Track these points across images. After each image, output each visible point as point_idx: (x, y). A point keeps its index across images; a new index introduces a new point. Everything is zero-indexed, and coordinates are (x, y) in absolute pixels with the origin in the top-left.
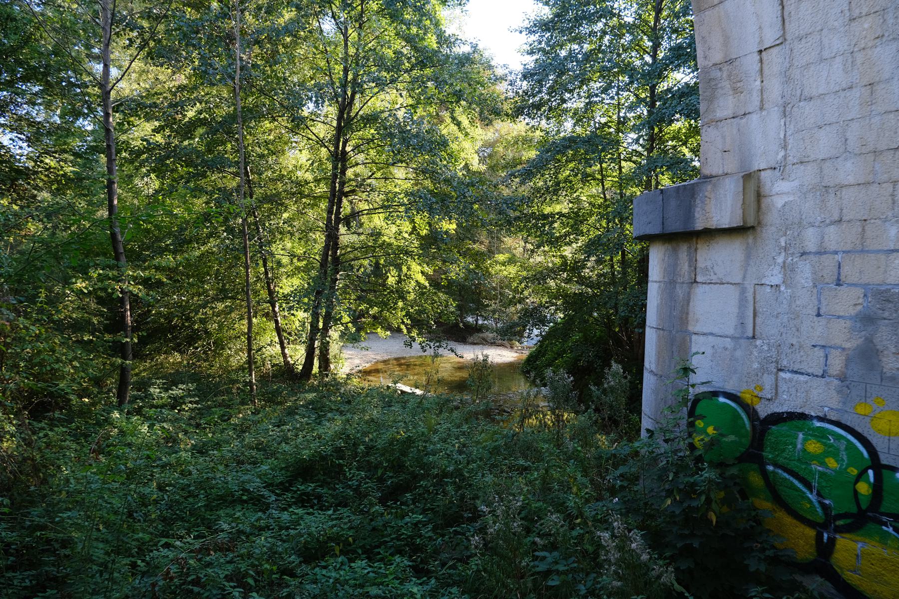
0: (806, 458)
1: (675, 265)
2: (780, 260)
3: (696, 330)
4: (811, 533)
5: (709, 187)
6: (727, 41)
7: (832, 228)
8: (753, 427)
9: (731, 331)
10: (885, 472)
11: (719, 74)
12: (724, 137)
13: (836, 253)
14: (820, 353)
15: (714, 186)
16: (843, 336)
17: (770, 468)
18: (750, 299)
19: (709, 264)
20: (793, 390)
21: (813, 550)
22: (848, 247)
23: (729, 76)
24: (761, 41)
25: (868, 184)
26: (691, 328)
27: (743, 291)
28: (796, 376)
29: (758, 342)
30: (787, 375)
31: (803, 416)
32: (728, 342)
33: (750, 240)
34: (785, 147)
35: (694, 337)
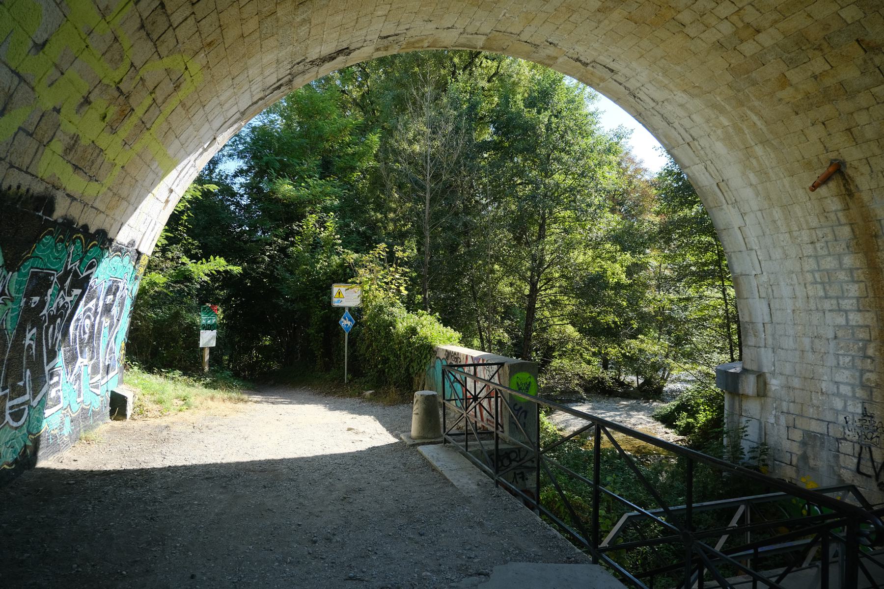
2: (774, 412)
6: (750, 314)
27: (760, 423)
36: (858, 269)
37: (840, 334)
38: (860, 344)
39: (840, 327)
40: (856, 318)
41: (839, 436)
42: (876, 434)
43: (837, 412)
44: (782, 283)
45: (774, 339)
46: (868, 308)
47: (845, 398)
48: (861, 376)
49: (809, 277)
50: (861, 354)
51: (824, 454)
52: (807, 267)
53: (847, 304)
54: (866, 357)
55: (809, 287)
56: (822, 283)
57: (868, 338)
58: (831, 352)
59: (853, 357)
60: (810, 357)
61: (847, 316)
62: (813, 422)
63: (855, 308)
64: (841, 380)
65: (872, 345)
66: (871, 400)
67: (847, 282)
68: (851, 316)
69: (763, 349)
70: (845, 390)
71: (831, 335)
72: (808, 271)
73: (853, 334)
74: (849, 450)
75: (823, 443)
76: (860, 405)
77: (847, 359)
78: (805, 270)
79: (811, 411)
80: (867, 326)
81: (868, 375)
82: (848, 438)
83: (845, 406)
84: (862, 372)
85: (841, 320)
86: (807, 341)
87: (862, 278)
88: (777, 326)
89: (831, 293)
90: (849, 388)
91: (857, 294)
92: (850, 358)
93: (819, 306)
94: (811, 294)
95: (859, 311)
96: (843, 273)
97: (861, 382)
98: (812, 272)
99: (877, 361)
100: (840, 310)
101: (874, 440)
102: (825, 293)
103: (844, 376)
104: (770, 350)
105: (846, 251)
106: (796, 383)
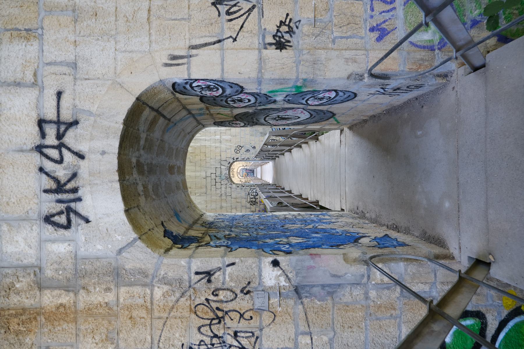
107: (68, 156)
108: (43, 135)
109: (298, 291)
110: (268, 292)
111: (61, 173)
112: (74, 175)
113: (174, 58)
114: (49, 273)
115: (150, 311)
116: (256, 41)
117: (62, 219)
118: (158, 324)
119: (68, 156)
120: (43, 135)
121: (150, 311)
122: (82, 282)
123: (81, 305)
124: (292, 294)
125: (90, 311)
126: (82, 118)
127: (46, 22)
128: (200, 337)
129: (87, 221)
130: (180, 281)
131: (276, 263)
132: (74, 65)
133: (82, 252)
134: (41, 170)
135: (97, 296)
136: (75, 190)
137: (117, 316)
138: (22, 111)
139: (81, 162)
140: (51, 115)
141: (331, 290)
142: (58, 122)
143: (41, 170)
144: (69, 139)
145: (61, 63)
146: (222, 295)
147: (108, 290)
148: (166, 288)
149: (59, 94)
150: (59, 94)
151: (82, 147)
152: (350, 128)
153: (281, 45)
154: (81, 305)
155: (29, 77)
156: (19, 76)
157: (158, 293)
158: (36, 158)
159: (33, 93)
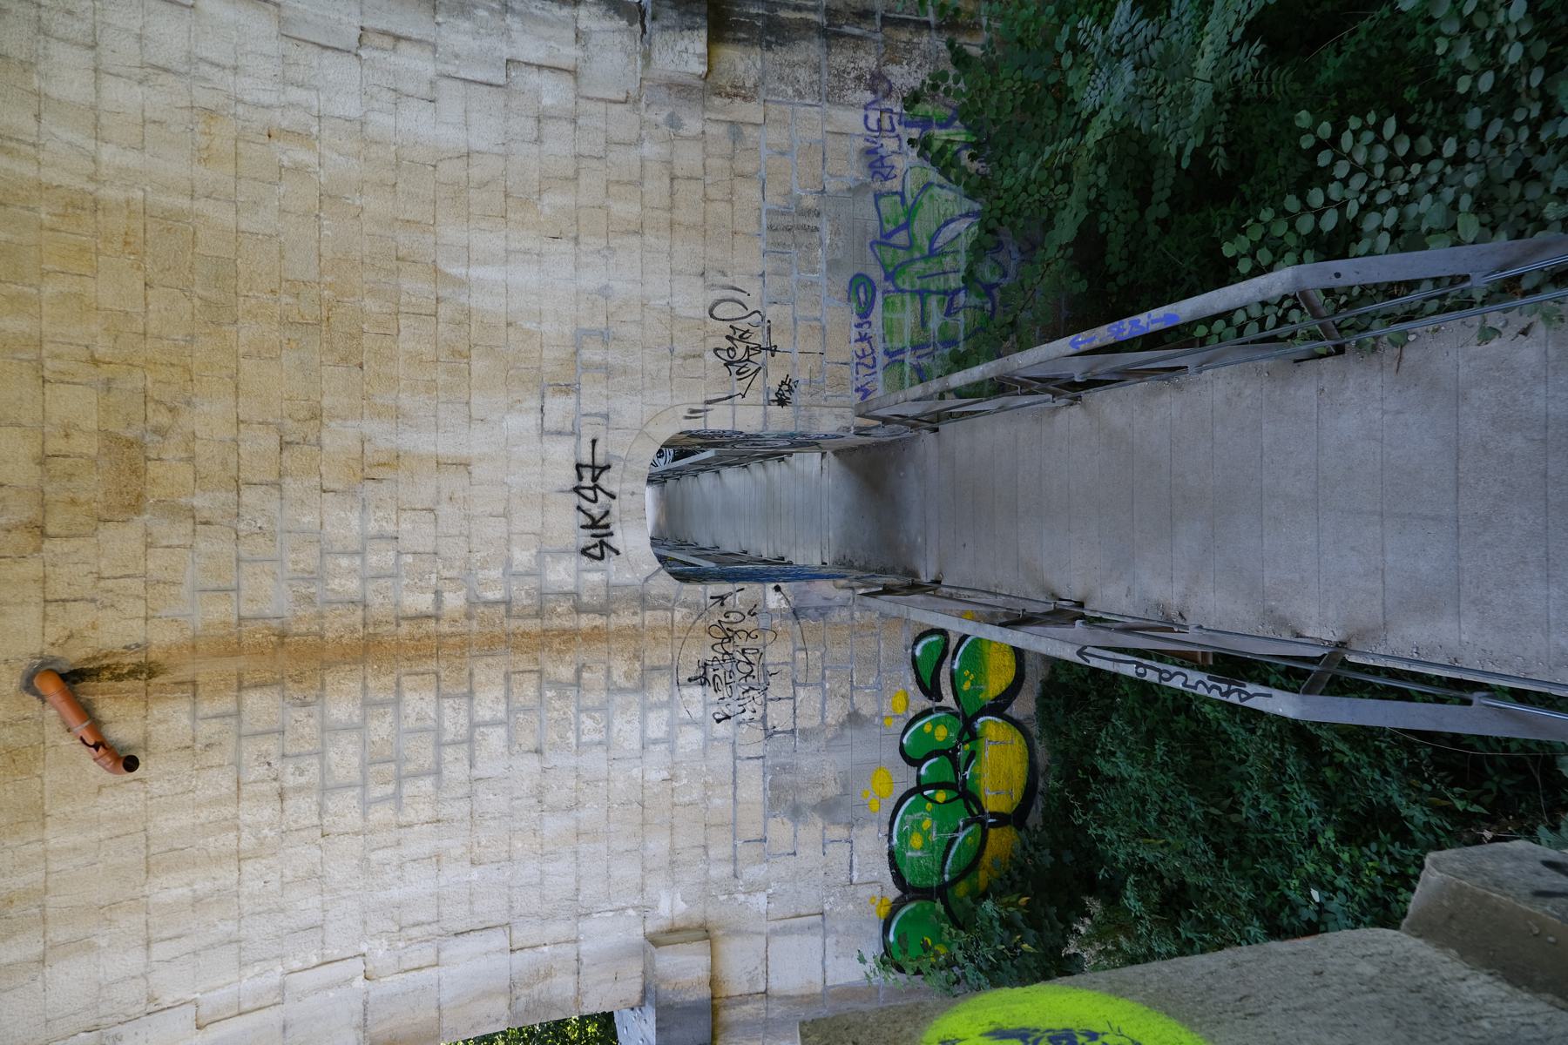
0: (927, 846)
1: (745, 1023)
2: (741, 898)
3: (820, 982)
4: (992, 831)
5: (663, 987)
6: (487, 994)
7: (711, 853)
8: (911, 900)
9: (818, 940)
10: (923, 782)
11: (523, 999)
12: (599, 983)
13: (735, 846)
14: (830, 847)
15: (662, 980)
16: (812, 831)
17: (947, 877)
18: (782, 923)
19: (745, 978)
20: (869, 867)
21: (1007, 829)
22: (730, 836)
23: (529, 986)
24: (501, 951)
25: (672, 827)
26: (819, 989)
27: (775, 932)
28: (855, 866)
29: (827, 908)
30: (855, 874)
31: (891, 855)
32: (830, 940)
33: (719, 933)
34: (624, 909)
35: (829, 983)
36: (365, 687)
37: (530, 742)
38: (549, 694)
39: (510, 741)
40: (489, 703)
41: (760, 734)
42: (738, 656)
43: (709, 740)
44: (396, 893)
45: (551, 917)
46: (465, 673)
47: (674, 726)
48: (621, 690)
49: (381, 814)
50: (572, 693)
51: (806, 763)
52: (353, 819)
53: (454, 721)
54: (577, 682)
55: (410, 815)
56: (400, 780)
57: (534, 676)
58: (573, 762)
59: (580, 710)
60: (590, 814)
61: (486, 724)
62: (743, 794)
63: (463, 703)
64: (637, 735)
65: (549, 668)
66: (670, 668)
67: (398, 717)
68: (484, 713)
69: (584, 947)
70: (657, 725)
71: (533, 762)
72: (364, 815)
73: (526, 710)
74: (786, 707)
75: (783, 768)
76: (685, 691)
77: (588, 723)
78: (359, 823)
79: (720, 801)
80: (507, 677)
81: (618, 676)
82: (760, 712)
83: (693, 723)
84: (612, 689)
85: (495, 739)
86: (555, 825)
87: (389, 680)
88: (518, 909)
89: (426, 759)
90: (652, 716)
91: (430, 696)
92: (583, 717)
93: (461, 792)
94: (426, 812)
95: (470, 695)
96: (374, 724)
97: (635, 691)
98: (366, 804)
99: (583, 658)
100: (470, 740)
101: (751, 658)
102: (428, 774)
103: (626, 729)
104: (584, 925)
105: (315, 709)
106: (658, 845)
107: (602, 497)
108: (580, 478)
109: (796, 613)
110: (771, 614)
111: (596, 511)
112: (607, 513)
113: (693, 411)
114: (585, 599)
115: (671, 632)
116: (761, 399)
117: (597, 552)
118: (678, 643)
119: (602, 497)
120: (580, 478)
121: (671, 632)
122: (614, 606)
123: (613, 627)
124: (791, 615)
125: (620, 633)
126: (614, 463)
127: (583, 379)
128: (714, 654)
129: (617, 553)
130: (698, 604)
131: (777, 589)
132: (607, 417)
133: (613, 580)
134: (579, 508)
135: (626, 619)
136: (607, 526)
137: (642, 636)
138: (562, 456)
139: (613, 502)
140: (587, 460)
141: (823, 612)
142: (593, 467)
143: (579, 508)
144: (602, 481)
145: (596, 415)
146: (732, 617)
147: (635, 613)
148: (685, 611)
149: (594, 442)
150: (594, 442)
151: (614, 489)
152: (836, 453)
153: (782, 402)
154: (613, 627)
155: (569, 428)
156: (560, 425)
157: (678, 616)
158: (575, 498)
159: (573, 440)
